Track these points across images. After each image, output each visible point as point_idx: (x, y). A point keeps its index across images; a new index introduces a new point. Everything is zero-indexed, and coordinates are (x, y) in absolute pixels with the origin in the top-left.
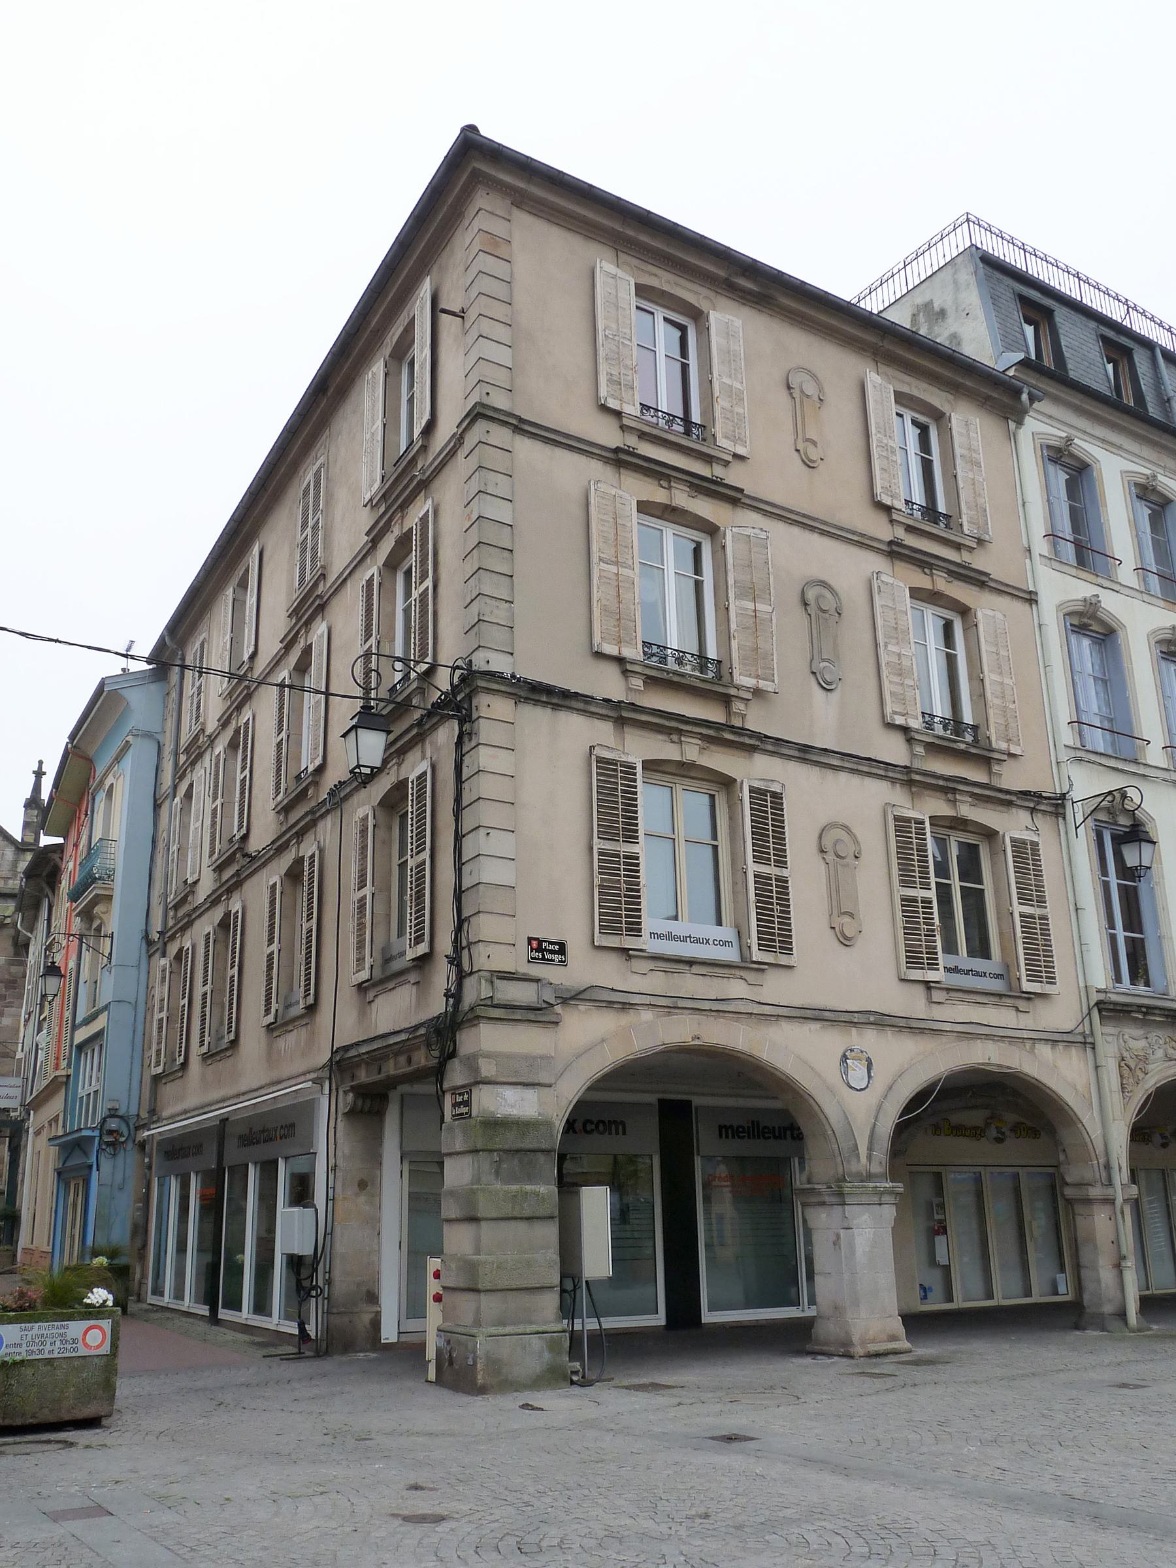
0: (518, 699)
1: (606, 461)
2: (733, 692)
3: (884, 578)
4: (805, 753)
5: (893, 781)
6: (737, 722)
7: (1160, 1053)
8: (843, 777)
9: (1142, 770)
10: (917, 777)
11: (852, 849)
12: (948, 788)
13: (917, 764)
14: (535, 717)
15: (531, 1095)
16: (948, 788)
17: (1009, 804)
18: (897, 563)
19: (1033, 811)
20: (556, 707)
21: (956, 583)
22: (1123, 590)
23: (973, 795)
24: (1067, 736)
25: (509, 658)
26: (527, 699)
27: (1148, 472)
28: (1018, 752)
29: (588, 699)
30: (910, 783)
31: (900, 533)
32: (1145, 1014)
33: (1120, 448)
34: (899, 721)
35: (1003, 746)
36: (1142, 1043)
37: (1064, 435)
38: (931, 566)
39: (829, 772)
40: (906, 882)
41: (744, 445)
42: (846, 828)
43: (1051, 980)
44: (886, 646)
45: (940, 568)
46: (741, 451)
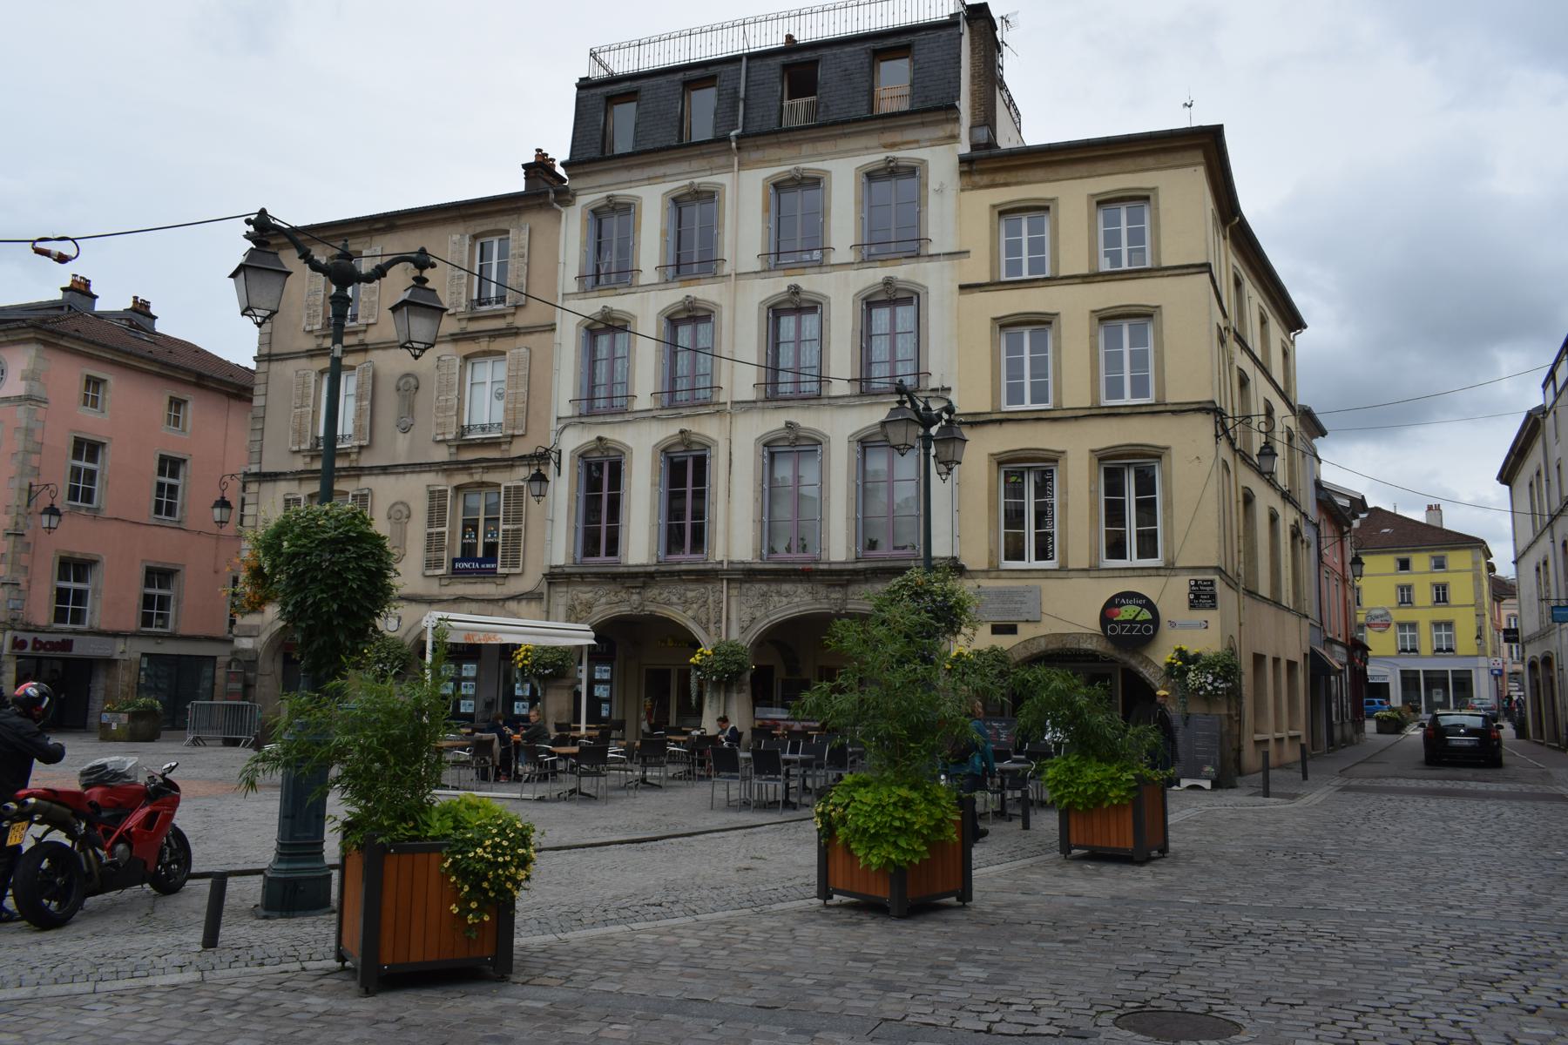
0: (260, 482)
1: (307, 357)
2: (349, 451)
3: (443, 358)
4: (385, 470)
5: (437, 471)
6: (354, 465)
7: (603, 600)
8: (408, 476)
9: (627, 417)
10: (445, 467)
11: (405, 512)
12: (466, 466)
13: (454, 458)
14: (268, 487)
15: (251, 640)
16: (466, 466)
17: (512, 466)
18: (460, 344)
19: (529, 465)
20: (275, 481)
21: (498, 340)
22: (640, 289)
23: (483, 468)
24: (566, 410)
25: (258, 466)
26: (264, 481)
27: (687, 182)
28: (521, 432)
29: (284, 474)
30: (445, 470)
31: (464, 324)
32: (582, 578)
33: (665, 176)
34: (440, 438)
35: (510, 432)
36: (590, 595)
37: (604, 194)
38: (478, 338)
39: (401, 476)
40: (430, 526)
41: (373, 316)
42: (402, 503)
43: (516, 565)
44: (438, 398)
45: (483, 337)
46: (371, 321)
